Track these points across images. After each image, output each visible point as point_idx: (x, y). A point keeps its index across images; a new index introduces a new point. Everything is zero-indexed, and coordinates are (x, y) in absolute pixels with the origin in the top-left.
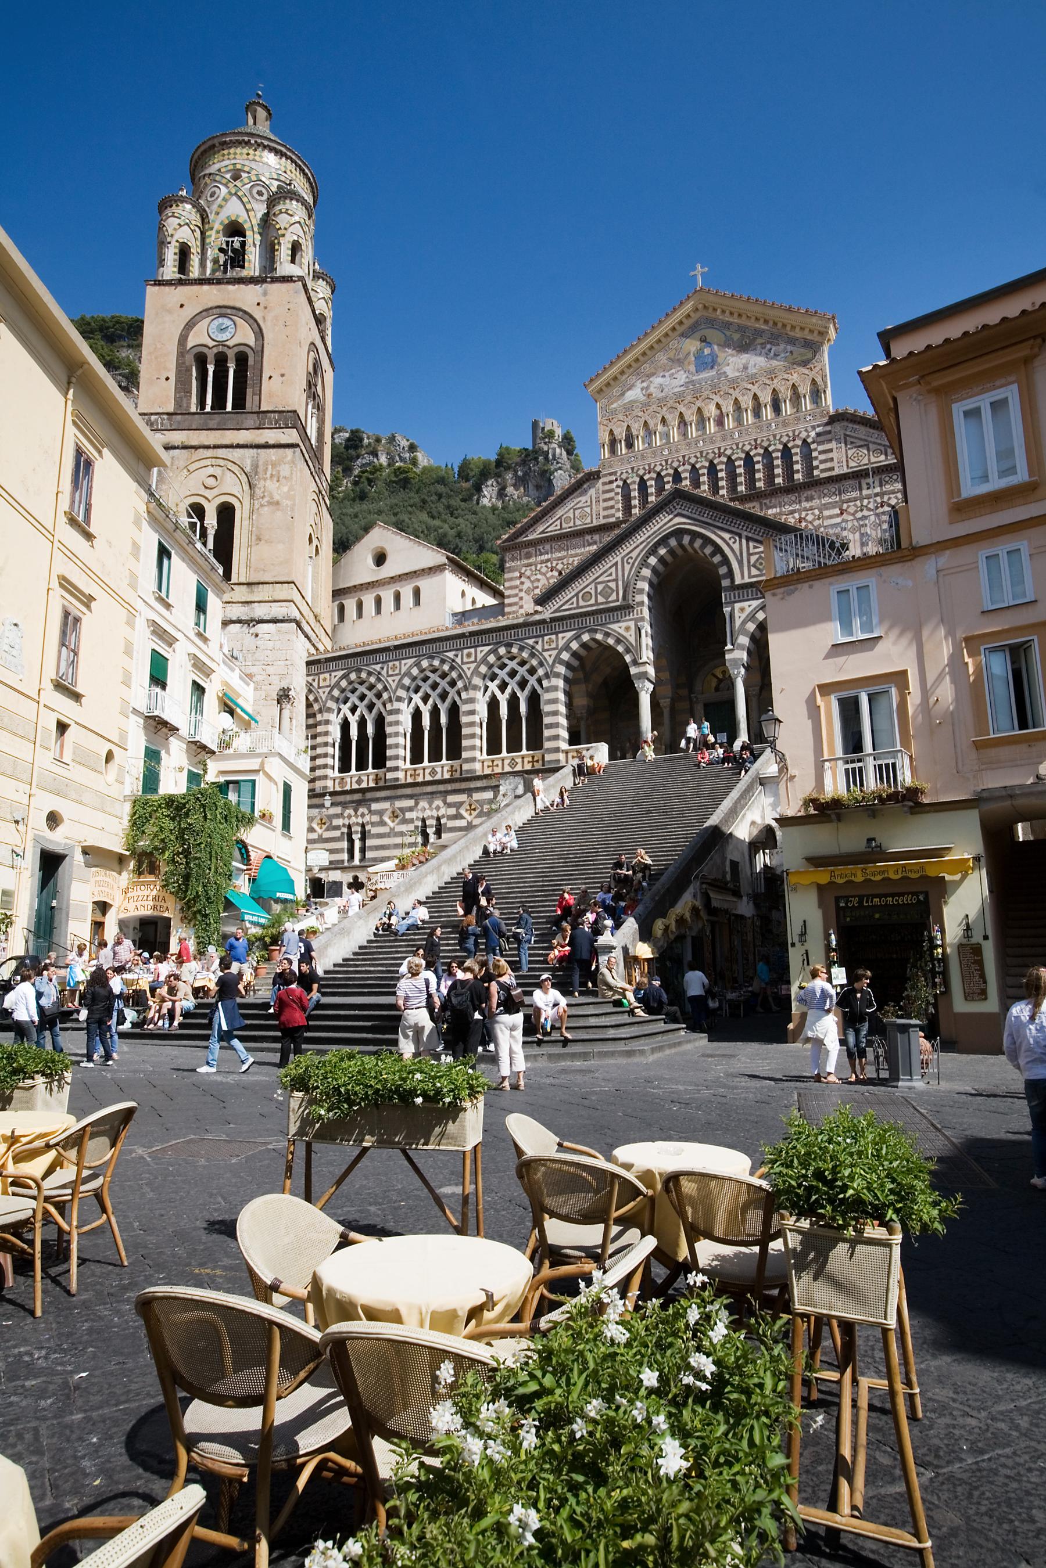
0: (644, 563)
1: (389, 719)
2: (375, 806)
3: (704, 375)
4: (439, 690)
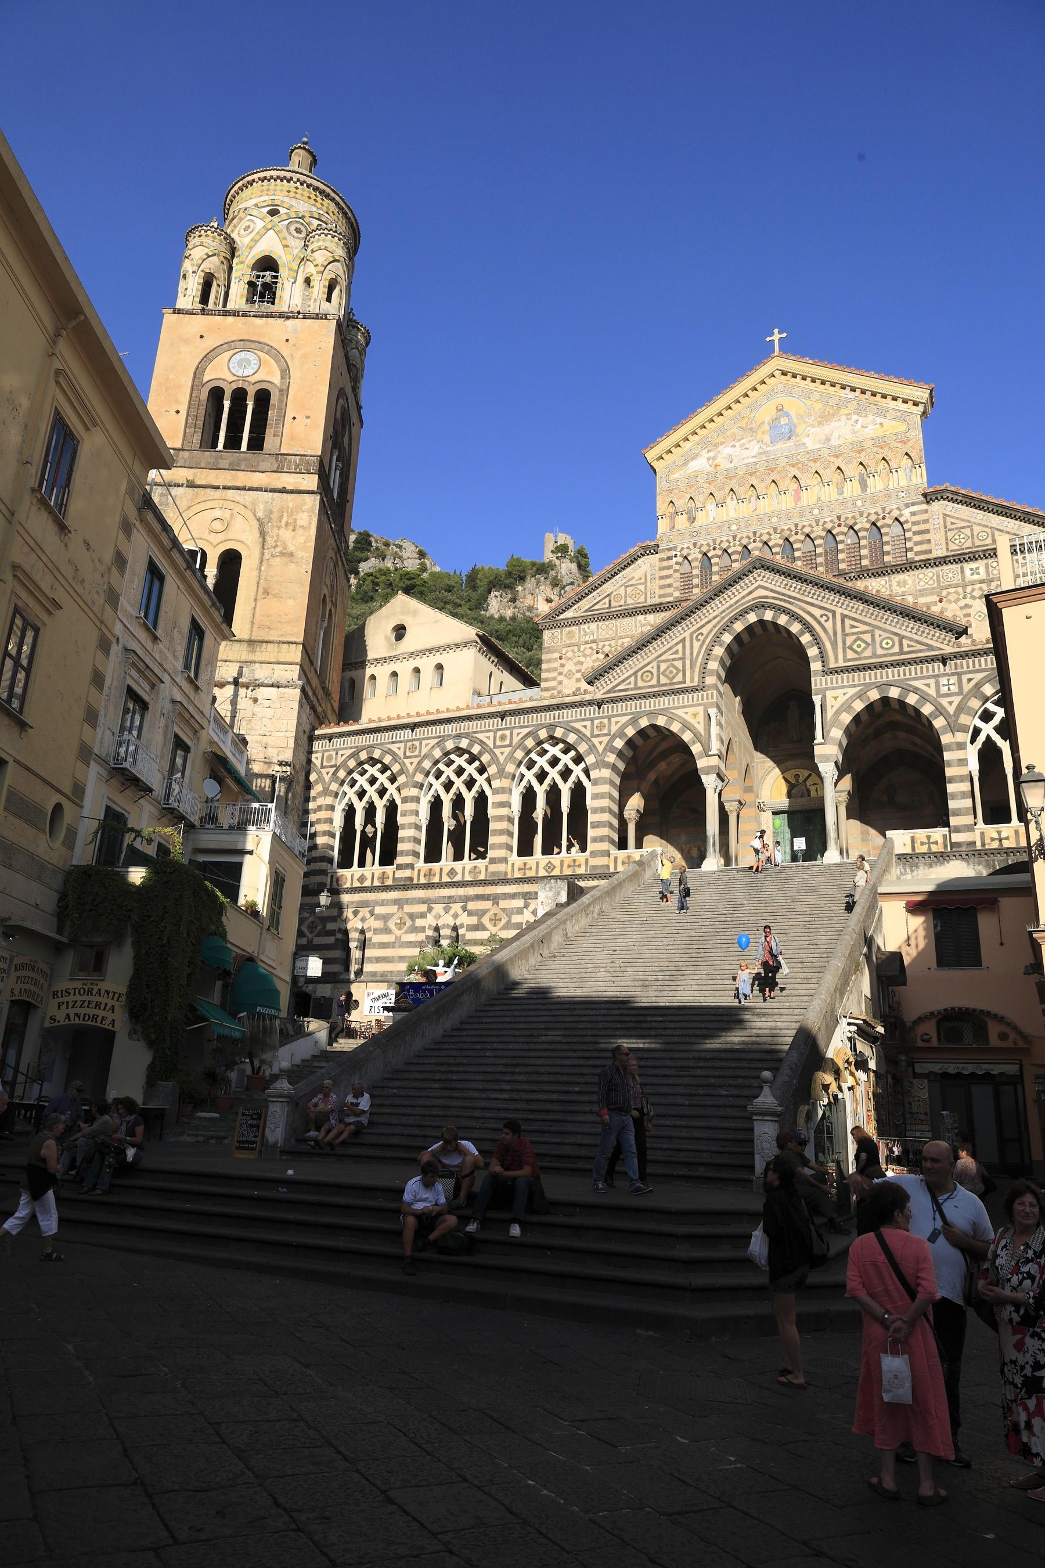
0: (716, 640)
2: (378, 910)
3: (780, 446)
4: (465, 776)
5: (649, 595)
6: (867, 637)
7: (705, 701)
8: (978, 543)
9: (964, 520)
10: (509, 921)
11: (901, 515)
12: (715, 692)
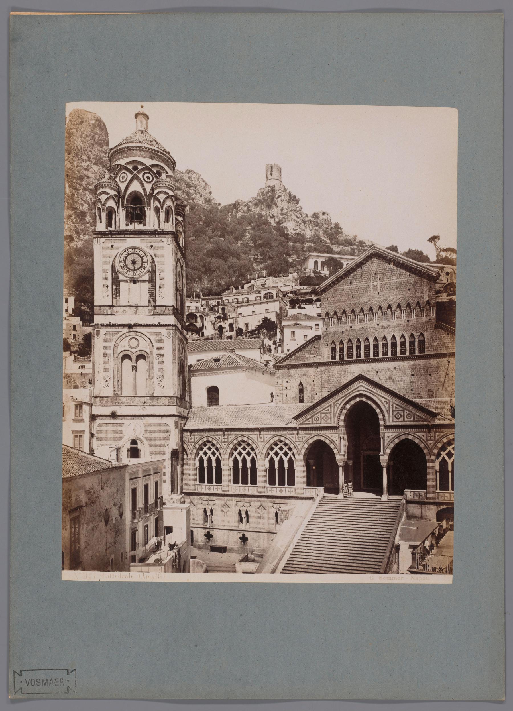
0: (344, 407)
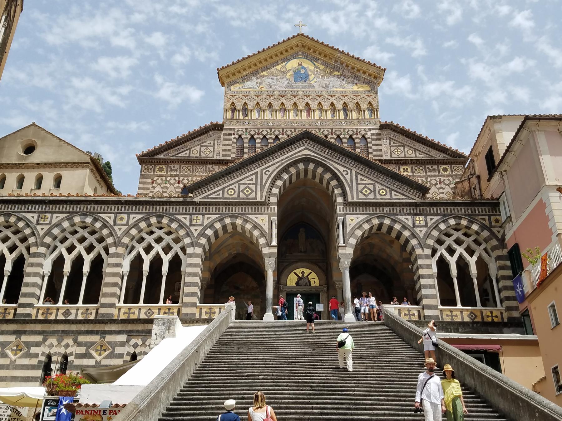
1: (29, 260)
3: (300, 84)
5: (215, 154)
6: (371, 187)
7: (269, 211)
8: (407, 155)
9: (400, 142)
10: (113, 351)
11: (366, 134)
12: (276, 207)
